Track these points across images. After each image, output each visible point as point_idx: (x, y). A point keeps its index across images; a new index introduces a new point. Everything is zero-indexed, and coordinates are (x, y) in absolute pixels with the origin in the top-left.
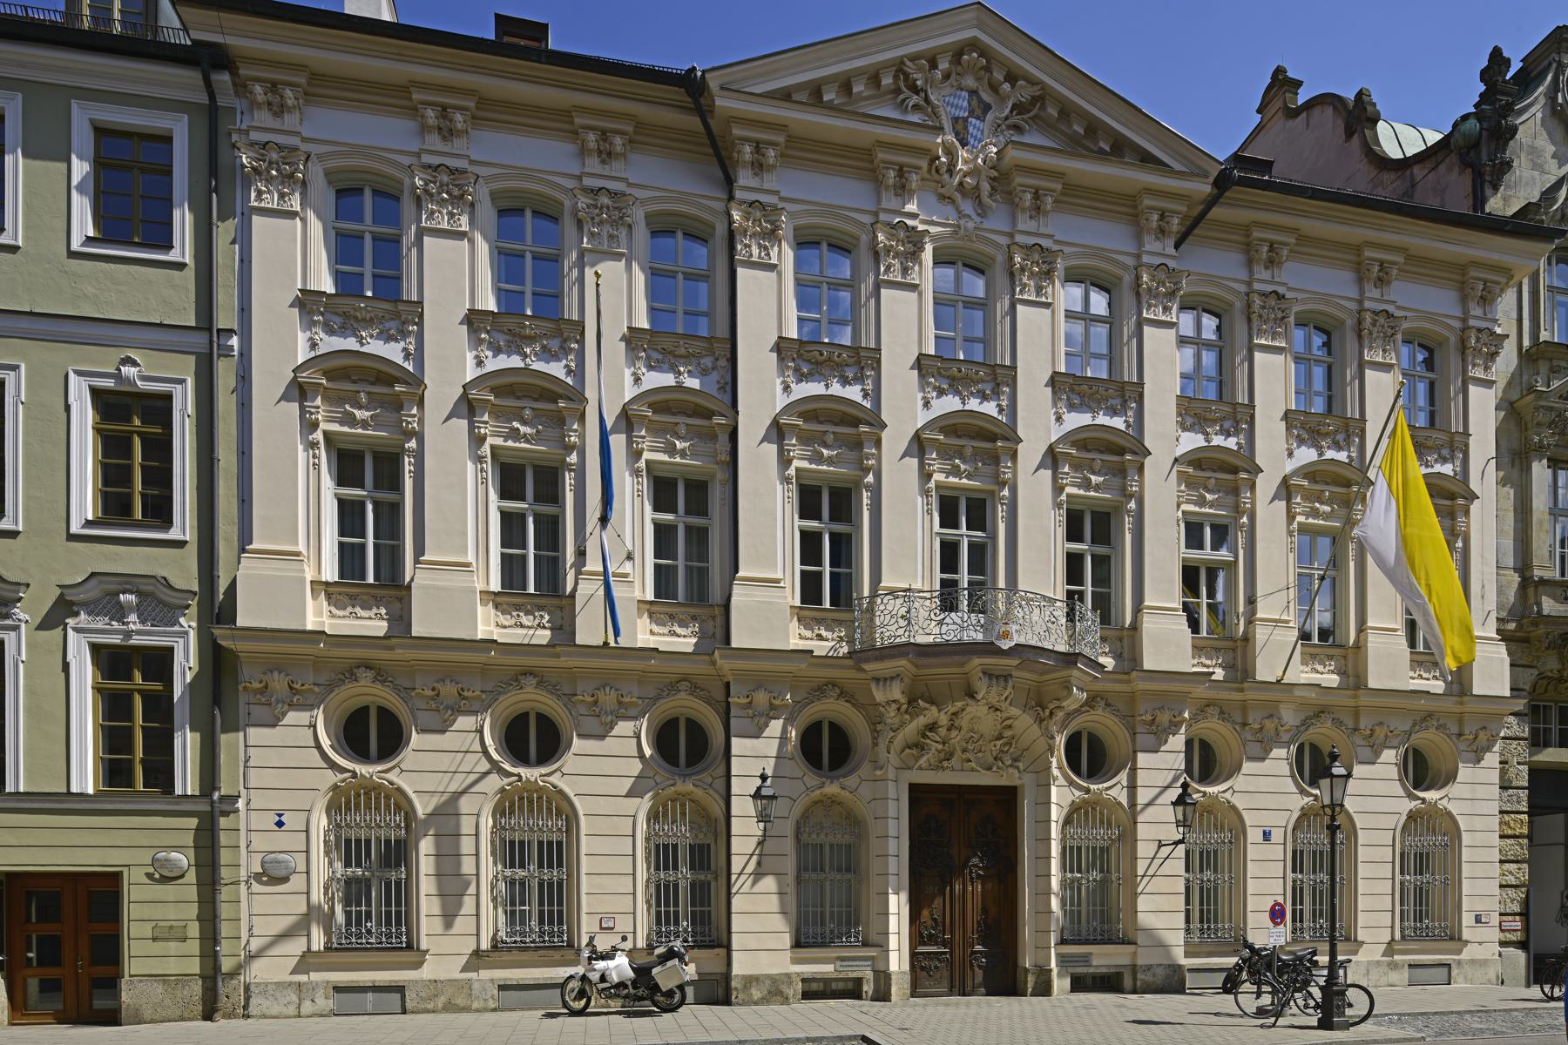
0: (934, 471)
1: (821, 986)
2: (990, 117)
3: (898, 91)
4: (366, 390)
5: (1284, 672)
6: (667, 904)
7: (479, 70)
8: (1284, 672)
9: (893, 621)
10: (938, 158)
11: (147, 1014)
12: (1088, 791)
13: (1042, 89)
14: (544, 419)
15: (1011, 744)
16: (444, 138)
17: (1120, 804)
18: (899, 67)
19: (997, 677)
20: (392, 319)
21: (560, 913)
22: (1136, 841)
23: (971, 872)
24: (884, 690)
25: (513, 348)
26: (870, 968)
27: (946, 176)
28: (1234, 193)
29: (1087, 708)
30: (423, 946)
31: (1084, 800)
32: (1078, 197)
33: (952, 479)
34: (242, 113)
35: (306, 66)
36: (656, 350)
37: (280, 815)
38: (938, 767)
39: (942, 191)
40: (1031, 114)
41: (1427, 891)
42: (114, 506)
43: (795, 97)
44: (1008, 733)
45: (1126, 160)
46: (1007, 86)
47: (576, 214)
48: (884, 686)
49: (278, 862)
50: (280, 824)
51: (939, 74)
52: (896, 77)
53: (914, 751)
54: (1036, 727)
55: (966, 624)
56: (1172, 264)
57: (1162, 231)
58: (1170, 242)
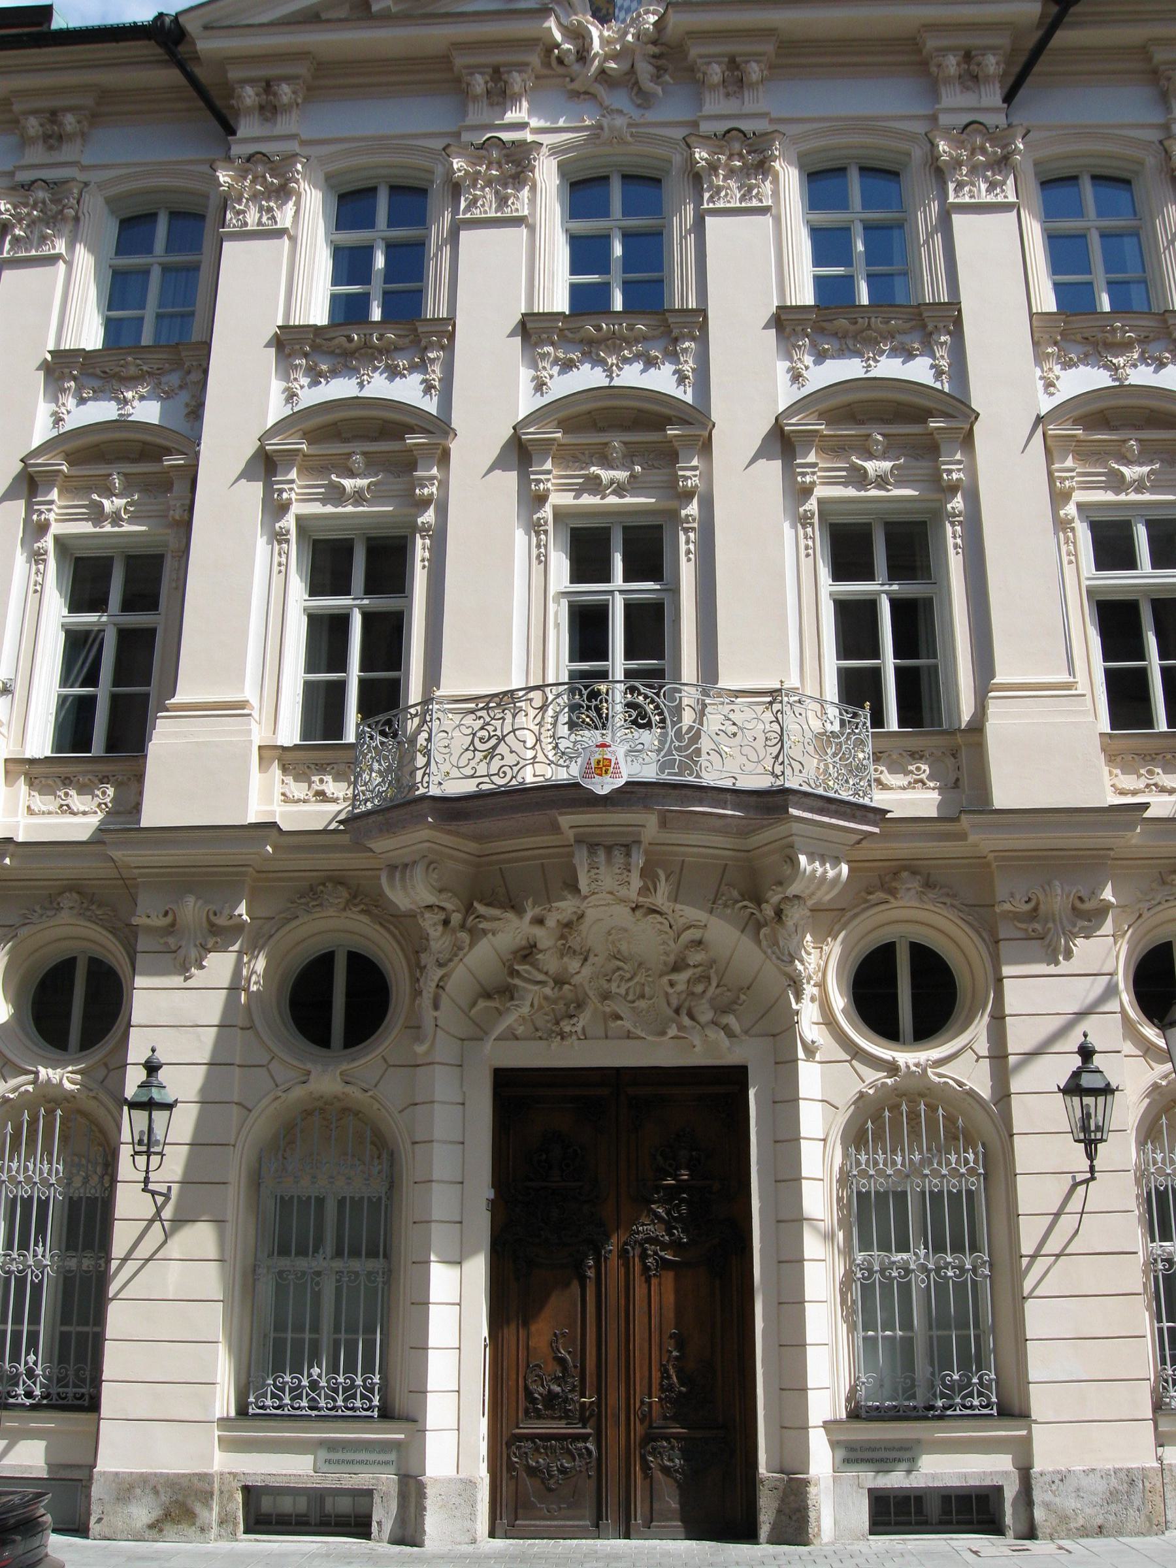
1: (302, 1505)
12: (892, 1068)
15: (709, 978)
17: (971, 1093)
23: (644, 1256)
24: (404, 888)
26: (392, 1469)
27: (576, 67)
29: (881, 895)
31: (895, 1088)
33: (587, 500)
39: (575, 86)
44: (696, 957)
48: (403, 879)
58: (993, 96)
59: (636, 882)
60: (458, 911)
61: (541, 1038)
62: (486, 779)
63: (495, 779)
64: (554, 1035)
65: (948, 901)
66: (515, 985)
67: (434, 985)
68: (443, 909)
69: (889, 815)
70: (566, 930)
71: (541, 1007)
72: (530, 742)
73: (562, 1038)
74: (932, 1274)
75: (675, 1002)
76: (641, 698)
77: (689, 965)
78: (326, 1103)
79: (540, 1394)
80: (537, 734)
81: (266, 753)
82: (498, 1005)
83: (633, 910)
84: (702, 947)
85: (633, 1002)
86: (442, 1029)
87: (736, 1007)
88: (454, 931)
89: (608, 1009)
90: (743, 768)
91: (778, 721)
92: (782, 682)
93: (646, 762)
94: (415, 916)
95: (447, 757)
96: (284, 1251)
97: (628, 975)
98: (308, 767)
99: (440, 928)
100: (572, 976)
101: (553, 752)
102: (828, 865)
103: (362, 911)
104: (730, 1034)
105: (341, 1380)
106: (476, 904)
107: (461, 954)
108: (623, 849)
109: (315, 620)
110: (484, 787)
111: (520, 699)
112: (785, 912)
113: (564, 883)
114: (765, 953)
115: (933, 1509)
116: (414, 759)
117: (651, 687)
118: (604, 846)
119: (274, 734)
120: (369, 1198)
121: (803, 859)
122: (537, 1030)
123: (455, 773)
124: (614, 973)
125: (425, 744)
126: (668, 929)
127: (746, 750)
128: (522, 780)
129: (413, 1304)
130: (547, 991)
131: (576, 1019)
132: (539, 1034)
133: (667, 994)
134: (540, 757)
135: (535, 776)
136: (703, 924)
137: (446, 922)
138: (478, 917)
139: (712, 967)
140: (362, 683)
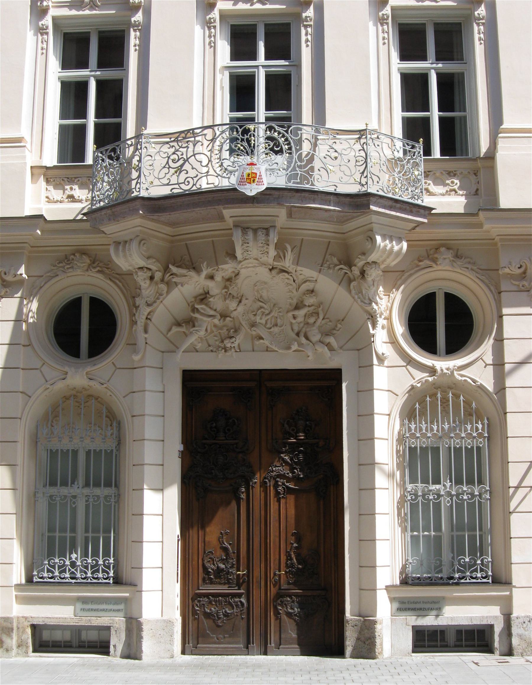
1: (67, 636)
12: (432, 371)
15: (318, 314)
17: (481, 387)
23: (276, 486)
24: (125, 256)
26: (122, 614)
29: (428, 262)
31: (433, 384)
44: (310, 300)
48: (124, 250)
59: (272, 252)
60: (159, 271)
61: (212, 351)
62: (177, 186)
63: (183, 186)
64: (220, 349)
65: (469, 266)
66: (196, 318)
67: (144, 317)
68: (150, 269)
69: (433, 212)
70: (228, 283)
71: (212, 332)
72: (205, 161)
73: (226, 351)
74: (454, 498)
75: (296, 329)
76: (276, 134)
77: (305, 305)
78: (77, 392)
79: (212, 569)
80: (209, 157)
81: (36, 171)
82: (184, 330)
83: (271, 270)
84: (314, 294)
85: (271, 328)
86: (149, 345)
87: (335, 332)
88: (157, 283)
89: (254, 333)
90: (341, 179)
91: (364, 150)
92: (367, 125)
93: (279, 175)
94: (132, 274)
95: (151, 172)
96: (53, 483)
97: (267, 312)
98: (63, 180)
99: (148, 282)
100: (232, 312)
101: (220, 168)
102: (394, 242)
103: (99, 271)
104: (331, 349)
105: (90, 561)
106: (170, 266)
107: (161, 298)
108: (264, 231)
109: (66, 86)
110: (175, 191)
111: (197, 135)
112: (366, 272)
113: (227, 253)
114: (354, 298)
115: (451, 638)
116: (130, 173)
117: (282, 127)
118: (252, 229)
119: (41, 158)
120: (105, 450)
121: (378, 238)
122: (209, 346)
123: (156, 182)
124: (258, 310)
125: (137, 163)
126: (292, 282)
127: (343, 168)
128: (199, 187)
129: (133, 515)
130: (216, 321)
131: (234, 339)
132: (211, 348)
133: (291, 324)
134: (211, 172)
135: (208, 184)
136: (314, 279)
137: (152, 278)
138: (172, 275)
139: (320, 307)
140: (97, 126)
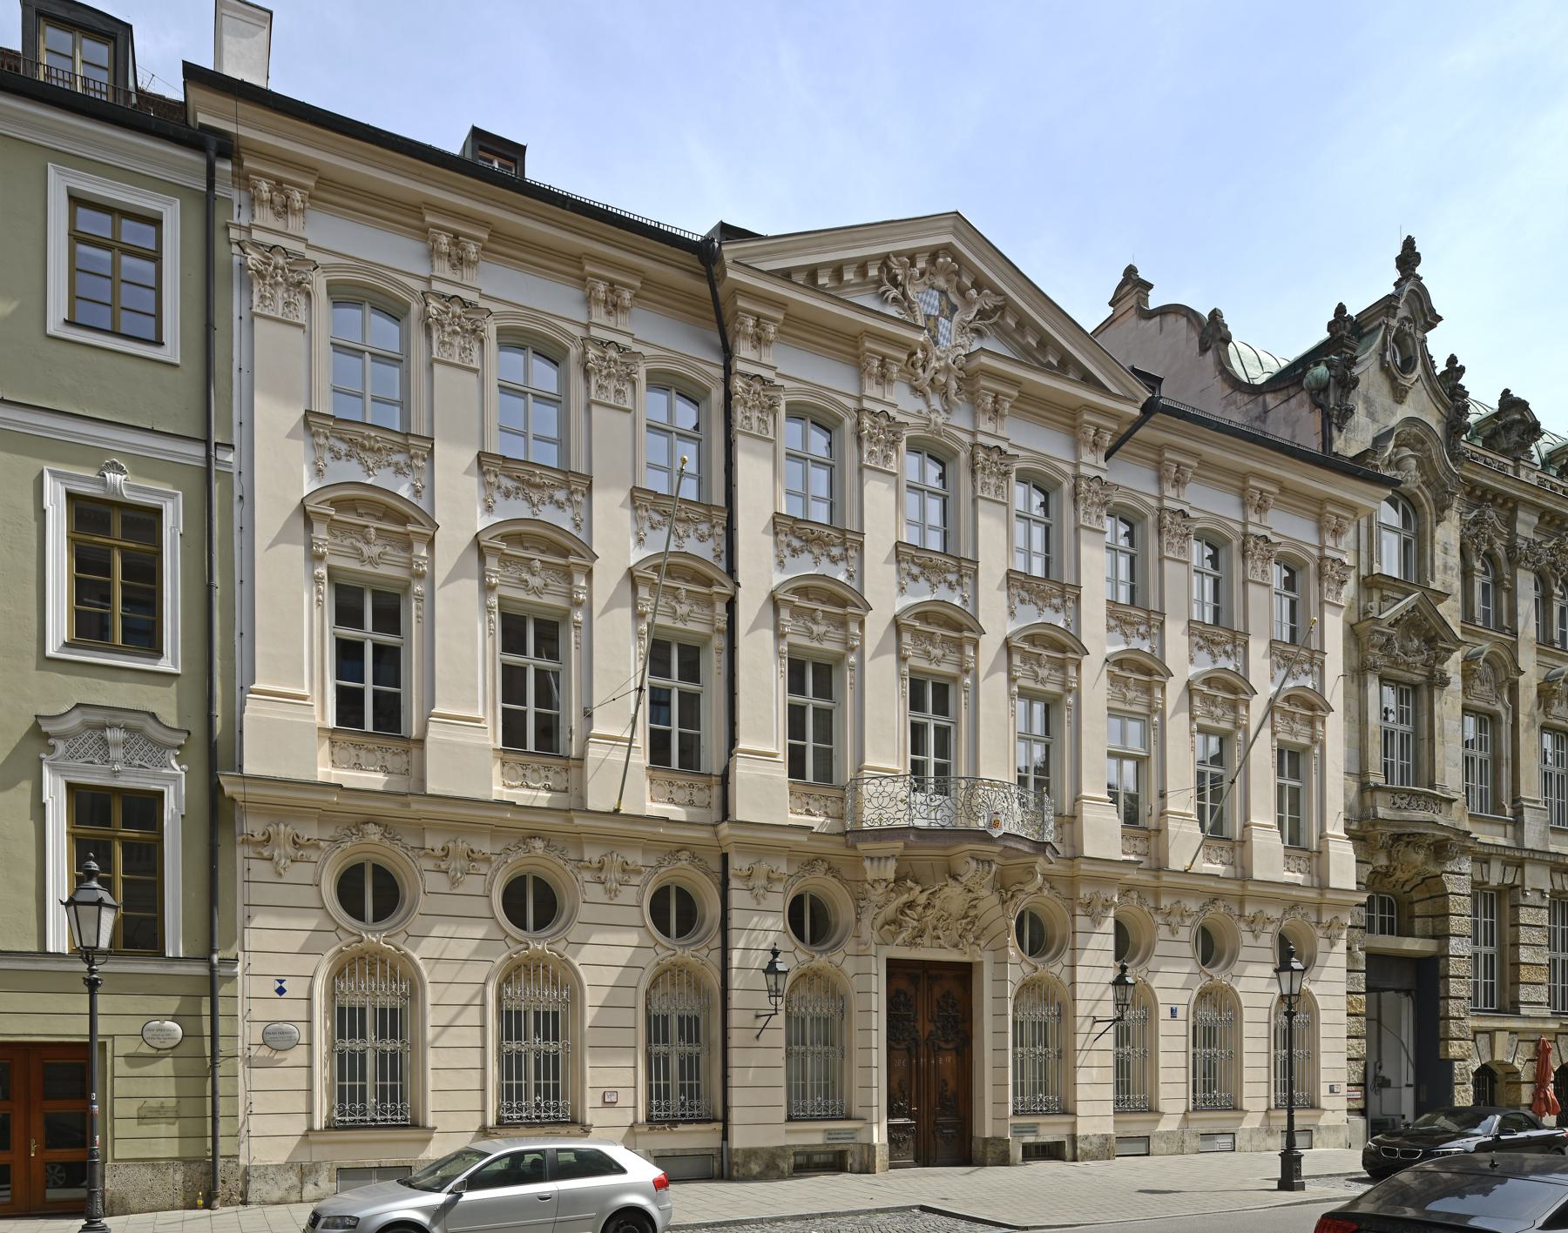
0: (909, 656)
2: (956, 318)
3: (879, 283)
4: (376, 526)
5: (1192, 863)
6: (547, 1077)
7: (498, 204)
8: (1192, 863)
9: (892, 803)
10: (915, 353)
11: (134, 1203)
13: (1004, 300)
14: (551, 572)
15: (974, 923)
16: (453, 266)
18: (885, 260)
19: (983, 862)
20: (400, 452)
21: (556, 1087)
22: (1075, 1017)
25: (520, 496)
27: (920, 371)
28: (1157, 418)
30: (430, 1124)
32: (1034, 405)
34: (240, 206)
35: (317, 170)
36: (657, 511)
37: (281, 982)
38: (911, 943)
40: (992, 321)
41: (1128, 1063)
42: (89, 628)
43: (795, 278)
44: (972, 913)
45: (1071, 376)
46: (973, 292)
47: (586, 364)
49: (282, 1033)
50: (281, 991)
51: (917, 272)
52: (880, 270)
53: (893, 928)
54: (999, 907)
55: (960, 812)
56: (1104, 477)
57: (1095, 444)
58: (1102, 455)
